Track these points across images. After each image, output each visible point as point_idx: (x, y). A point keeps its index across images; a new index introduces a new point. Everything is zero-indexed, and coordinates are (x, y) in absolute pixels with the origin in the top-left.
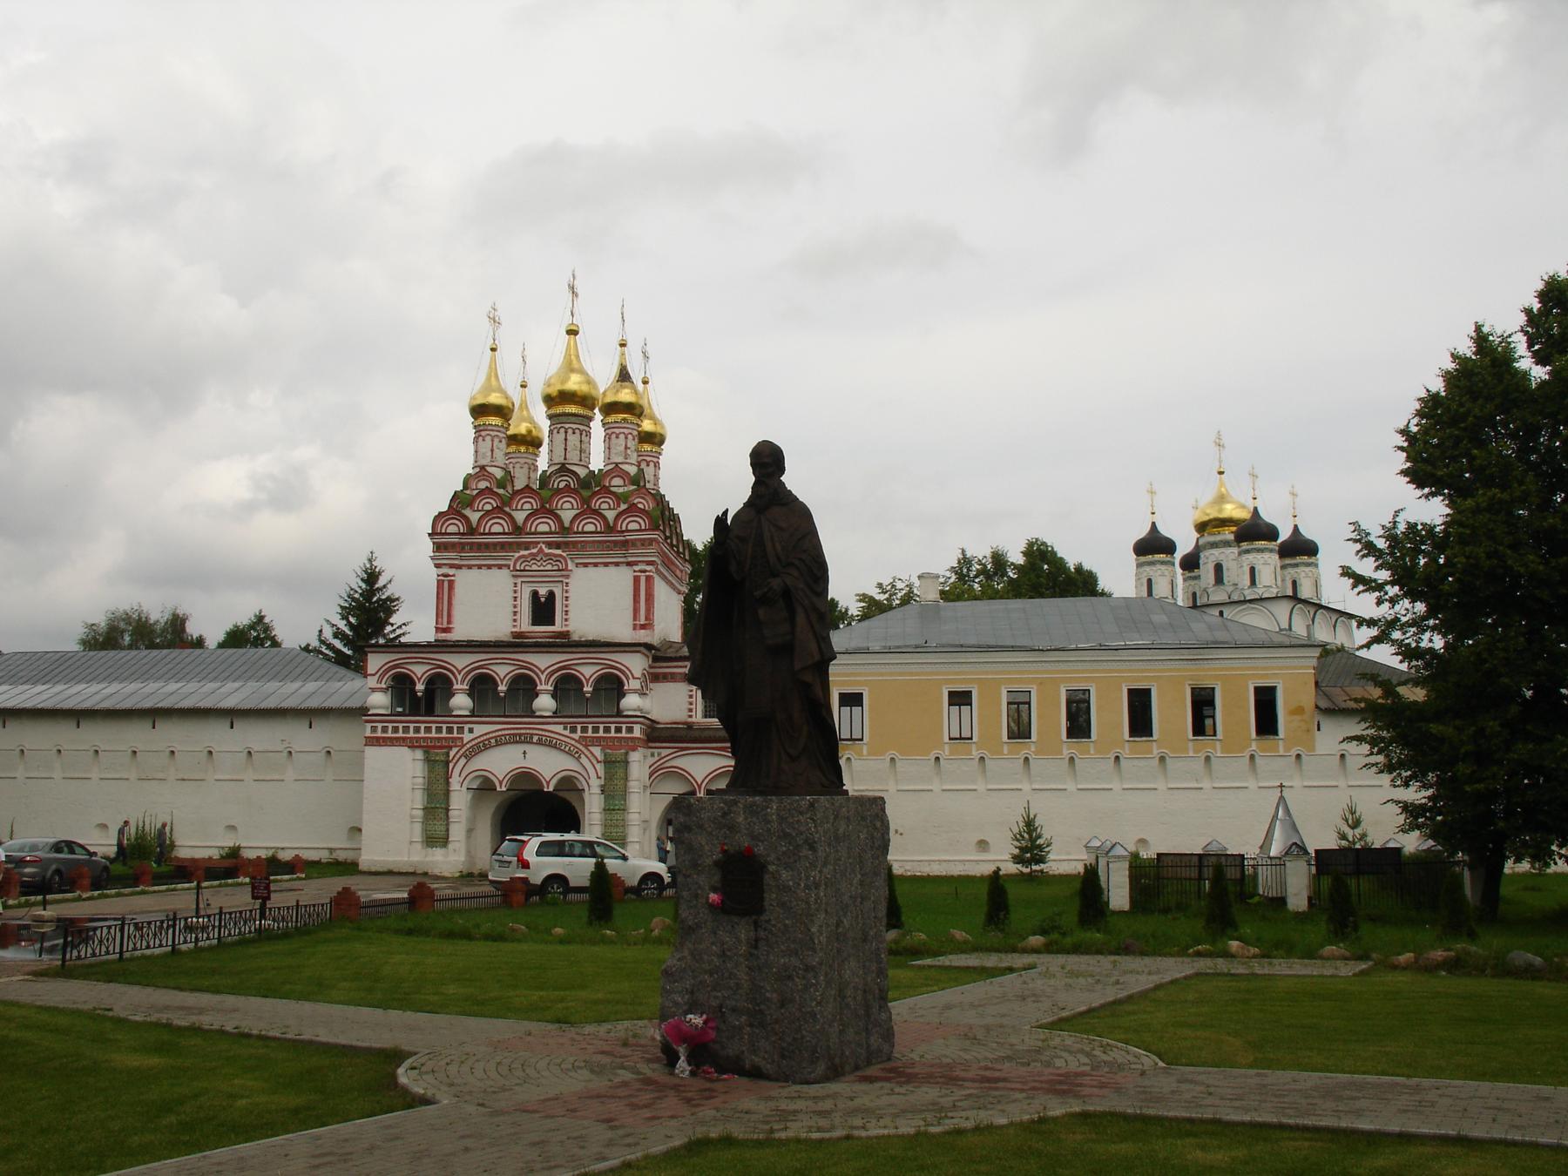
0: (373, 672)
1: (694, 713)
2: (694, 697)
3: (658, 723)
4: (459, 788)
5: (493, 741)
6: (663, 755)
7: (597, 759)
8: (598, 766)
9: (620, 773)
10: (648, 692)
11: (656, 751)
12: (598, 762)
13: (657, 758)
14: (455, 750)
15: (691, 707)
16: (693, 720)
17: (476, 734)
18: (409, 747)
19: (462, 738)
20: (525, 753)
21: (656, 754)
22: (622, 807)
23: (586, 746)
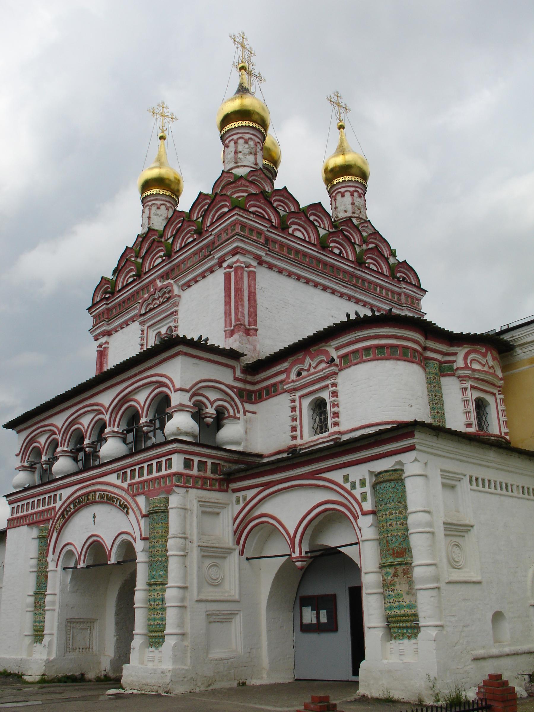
0: (18, 452)
1: (298, 432)
2: (298, 409)
3: (261, 456)
4: (54, 568)
5: (72, 506)
6: (248, 499)
7: (141, 512)
8: (142, 522)
9: (159, 526)
10: (238, 415)
11: (241, 494)
12: (143, 516)
13: (242, 505)
14: (51, 522)
15: (294, 423)
16: (299, 442)
17: (64, 498)
18: (29, 525)
19: (54, 508)
20: (94, 517)
21: (241, 500)
22: (160, 580)
23: (133, 496)
